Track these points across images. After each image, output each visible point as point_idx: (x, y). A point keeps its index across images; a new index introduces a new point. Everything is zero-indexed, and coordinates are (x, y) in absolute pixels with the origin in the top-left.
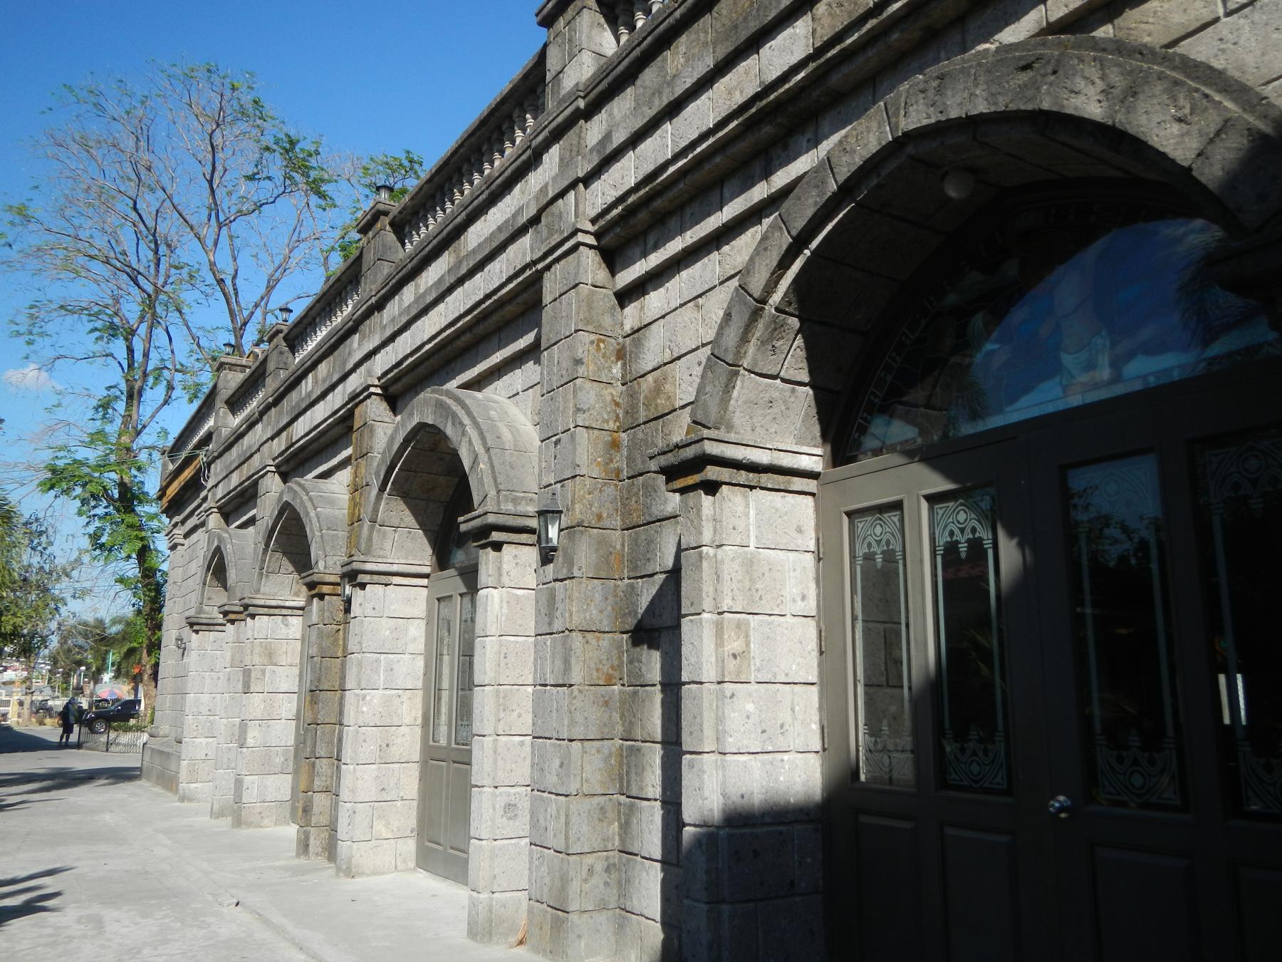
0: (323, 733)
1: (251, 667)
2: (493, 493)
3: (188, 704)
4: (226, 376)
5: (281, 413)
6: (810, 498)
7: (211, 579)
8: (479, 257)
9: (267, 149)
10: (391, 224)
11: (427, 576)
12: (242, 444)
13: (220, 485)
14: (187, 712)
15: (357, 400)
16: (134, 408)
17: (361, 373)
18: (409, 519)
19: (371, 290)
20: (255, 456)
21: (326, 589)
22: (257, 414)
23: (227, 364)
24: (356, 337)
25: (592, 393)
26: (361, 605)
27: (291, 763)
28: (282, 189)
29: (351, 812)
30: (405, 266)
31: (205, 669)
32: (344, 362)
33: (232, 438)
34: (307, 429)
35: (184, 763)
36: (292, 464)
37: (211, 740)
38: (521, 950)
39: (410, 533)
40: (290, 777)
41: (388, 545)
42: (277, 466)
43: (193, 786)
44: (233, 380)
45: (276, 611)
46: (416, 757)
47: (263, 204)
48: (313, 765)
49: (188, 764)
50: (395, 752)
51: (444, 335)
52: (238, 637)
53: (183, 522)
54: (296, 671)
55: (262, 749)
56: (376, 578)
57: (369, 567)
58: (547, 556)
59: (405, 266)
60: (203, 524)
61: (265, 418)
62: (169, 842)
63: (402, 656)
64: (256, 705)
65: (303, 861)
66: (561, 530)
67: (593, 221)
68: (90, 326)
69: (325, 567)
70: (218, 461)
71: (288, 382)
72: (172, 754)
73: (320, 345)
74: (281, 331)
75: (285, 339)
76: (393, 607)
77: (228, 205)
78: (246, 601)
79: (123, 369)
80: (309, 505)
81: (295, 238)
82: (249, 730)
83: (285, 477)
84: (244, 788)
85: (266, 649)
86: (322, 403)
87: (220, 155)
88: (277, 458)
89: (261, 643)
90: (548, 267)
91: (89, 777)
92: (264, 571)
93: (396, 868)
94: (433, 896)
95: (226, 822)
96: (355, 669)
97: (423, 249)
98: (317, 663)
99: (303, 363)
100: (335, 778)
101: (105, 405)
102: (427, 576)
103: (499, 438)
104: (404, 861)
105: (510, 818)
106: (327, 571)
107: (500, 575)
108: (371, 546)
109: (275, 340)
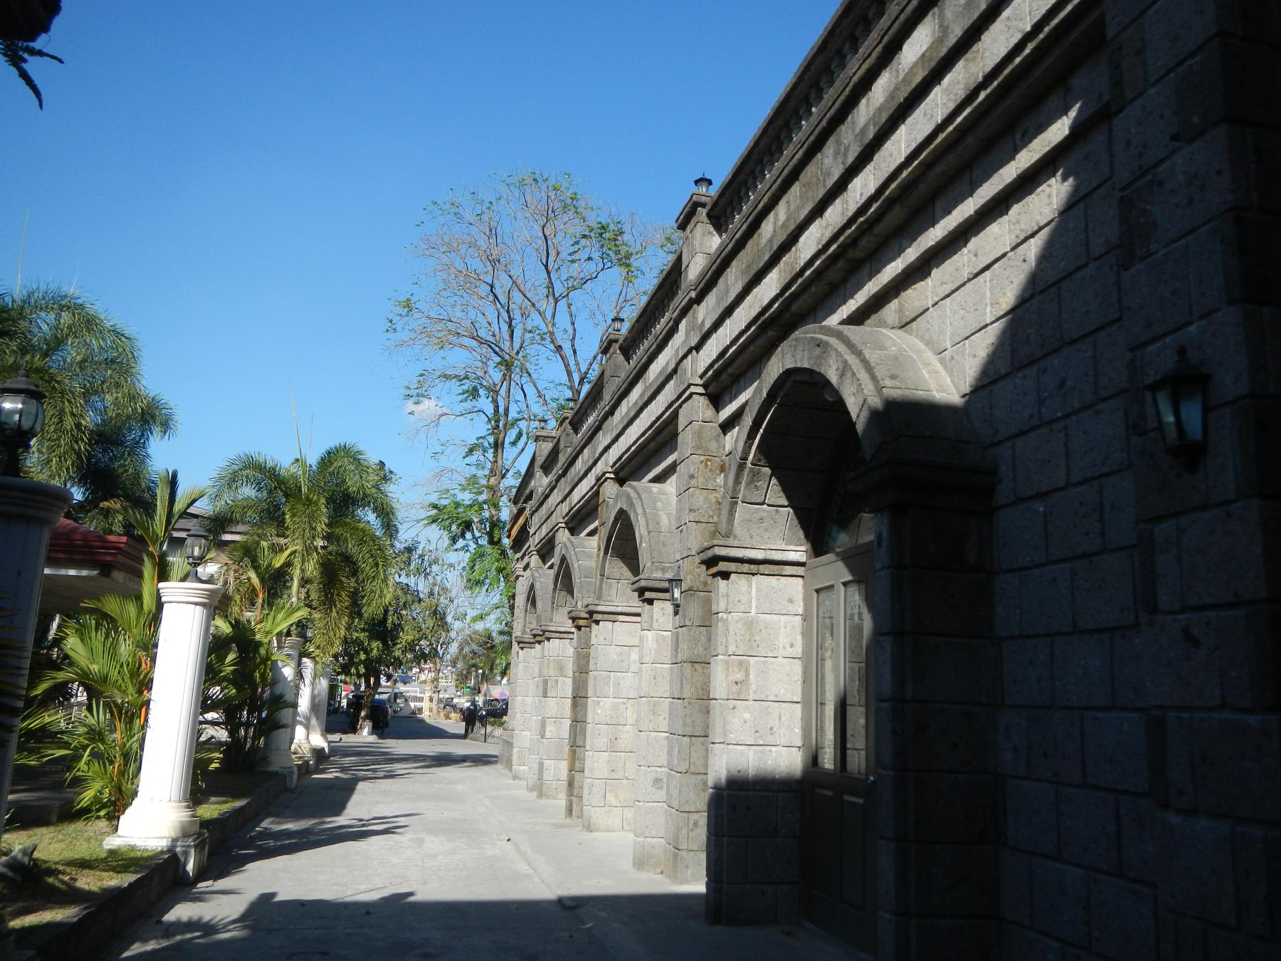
6: (800, 579)
10: (620, 348)
13: (537, 534)
23: (541, 436)
25: (701, 498)
34: (579, 498)
35: (515, 750)
38: (660, 877)
41: (614, 592)
43: (522, 768)
45: (565, 636)
56: (606, 616)
57: (600, 608)
58: (677, 607)
63: (626, 674)
64: (551, 707)
65: (568, 821)
66: (682, 593)
67: (701, 377)
70: (536, 514)
74: (567, 418)
75: (570, 423)
76: (619, 638)
84: (544, 769)
85: (558, 664)
89: (555, 660)
90: (680, 406)
91: (462, 759)
95: (535, 794)
103: (657, 524)
105: (657, 788)
107: (652, 621)
108: (602, 593)
109: (564, 424)
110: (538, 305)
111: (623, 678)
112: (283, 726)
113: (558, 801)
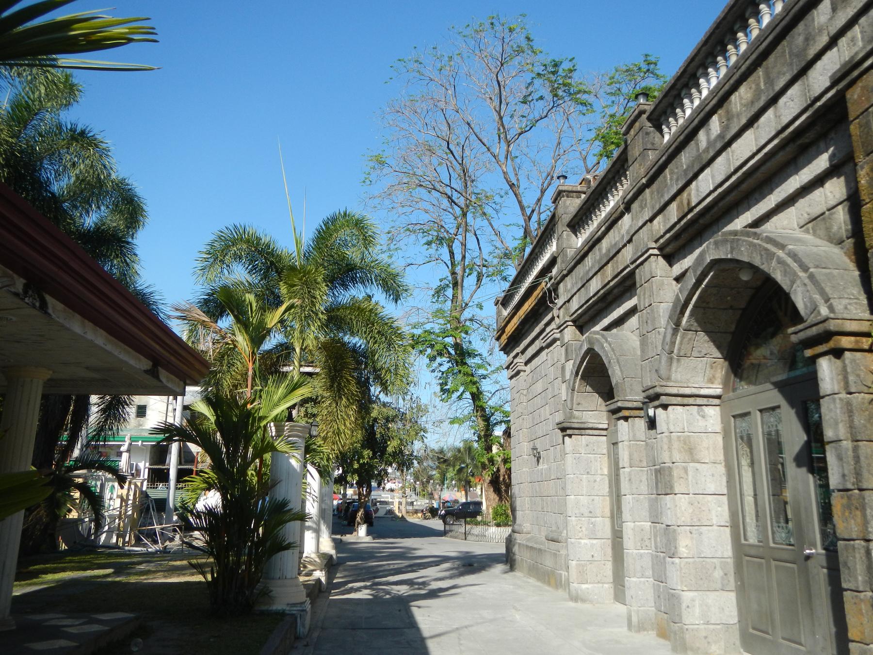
1: (671, 465)
3: (570, 505)
4: (565, 202)
7: (580, 384)
12: (600, 249)
15: (856, 73)
16: (459, 291)
22: (622, 207)
23: (564, 191)
27: (732, 578)
33: (586, 248)
36: (684, 237)
37: (595, 541)
40: (732, 596)
43: (584, 586)
44: (572, 205)
45: (691, 401)
49: (576, 565)
52: (634, 435)
53: (523, 352)
60: (554, 341)
61: (635, 206)
64: (683, 508)
68: (425, 240)
70: (568, 279)
71: (674, 146)
72: (545, 551)
74: (643, 112)
75: (649, 119)
77: (514, 126)
78: (658, 390)
79: (448, 267)
80: (769, 246)
81: (556, 154)
83: (670, 259)
84: (684, 606)
85: (685, 443)
87: (504, 93)
88: (662, 237)
89: (679, 437)
98: (847, 449)
101: (439, 291)
109: (637, 124)
110: (492, 150)
112: (288, 547)
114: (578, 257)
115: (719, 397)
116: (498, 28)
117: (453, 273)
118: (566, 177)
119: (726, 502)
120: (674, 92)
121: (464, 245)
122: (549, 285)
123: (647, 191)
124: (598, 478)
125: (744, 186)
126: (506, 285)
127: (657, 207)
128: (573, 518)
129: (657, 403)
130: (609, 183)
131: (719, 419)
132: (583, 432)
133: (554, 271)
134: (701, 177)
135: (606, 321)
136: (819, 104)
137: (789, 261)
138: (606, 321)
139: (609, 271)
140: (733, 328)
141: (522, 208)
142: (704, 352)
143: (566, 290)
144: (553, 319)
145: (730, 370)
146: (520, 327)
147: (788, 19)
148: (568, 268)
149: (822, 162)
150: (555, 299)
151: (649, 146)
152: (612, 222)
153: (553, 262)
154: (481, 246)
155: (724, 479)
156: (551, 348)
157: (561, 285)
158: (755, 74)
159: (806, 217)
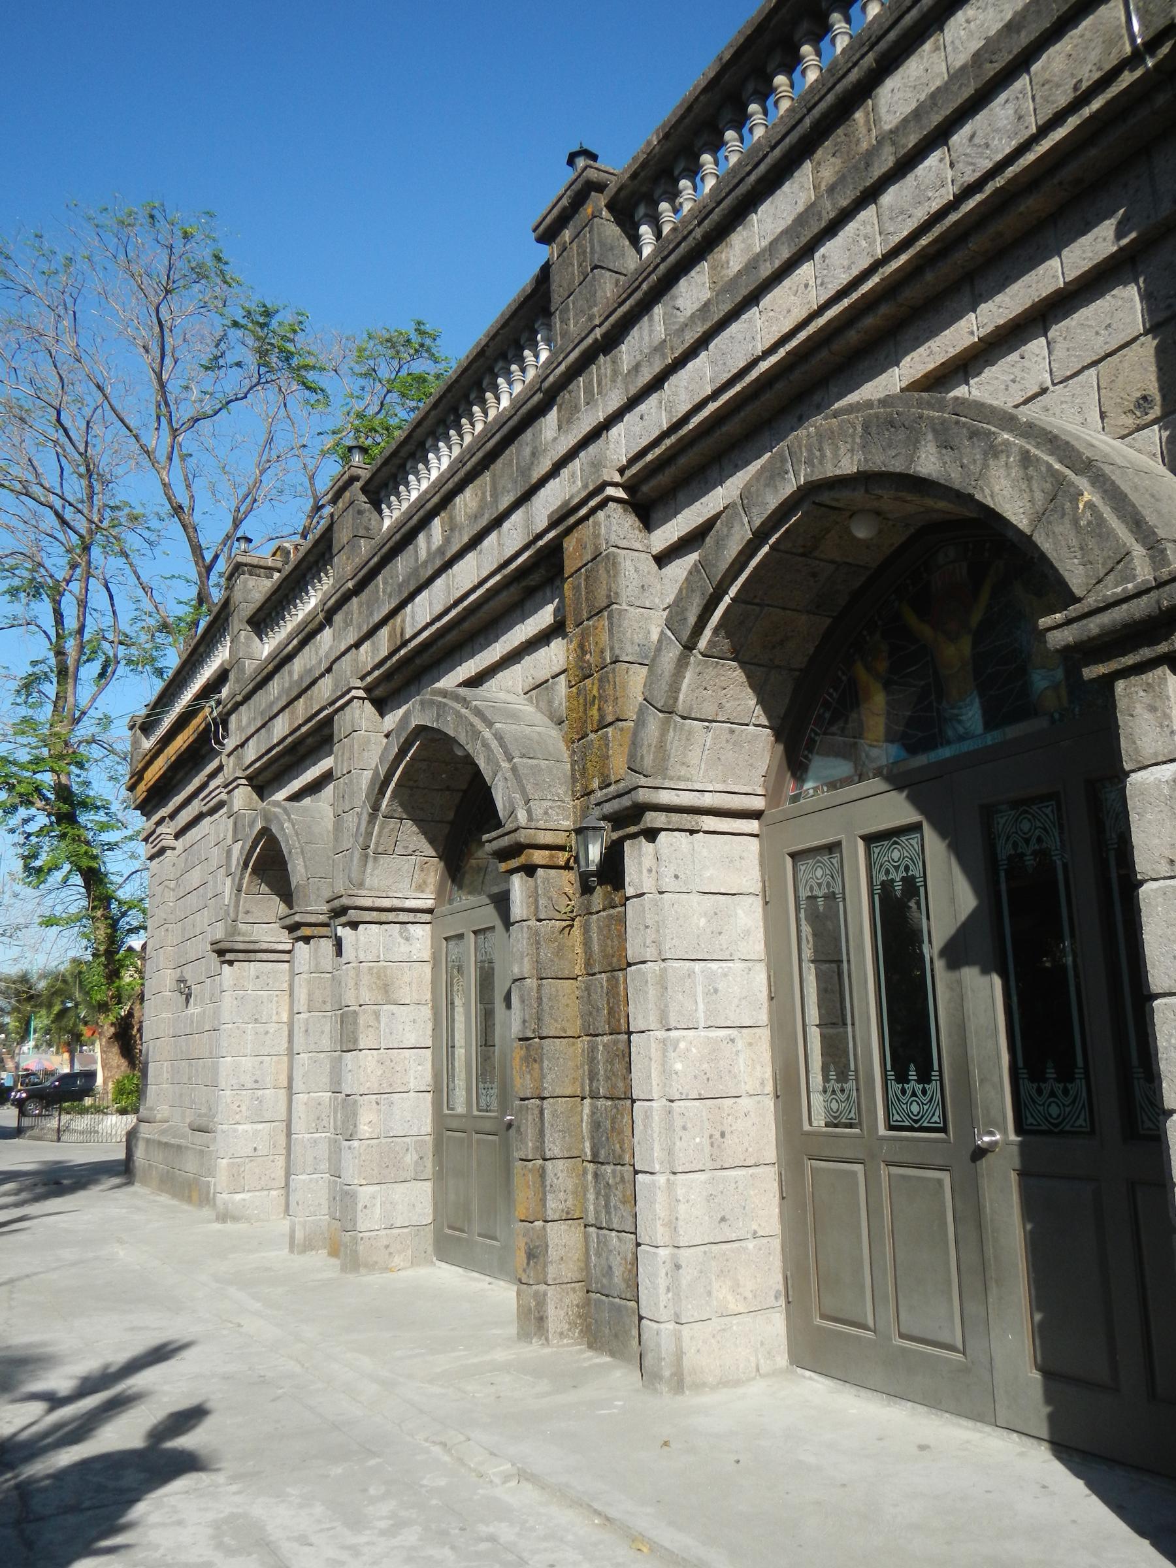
0: (554, 1114)
1: (357, 1008)
2: (1138, 551)
4: (245, 582)
5: (371, 605)
7: (250, 882)
8: (936, 119)
9: (236, 324)
10: (610, 207)
11: (756, 815)
12: (290, 673)
13: (251, 742)
14: (222, 1085)
15: (572, 520)
17: (573, 475)
18: (747, 702)
19: (591, 318)
20: (321, 682)
21: (539, 857)
22: (321, 616)
23: (246, 565)
24: (553, 415)
26: (650, 871)
27: (429, 1162)
28: (255, 380)
29: (669, 1265)
30: (685, 238)
31: (246, 1019)
32: (525, 471)
33: (270, 667)
34: (439, 609)
36: (398, 679)
37: (260, 1126)
39: (732, 731)
40: (428, 1187)
41: (694, 756)
42: (367, 689)
43: (238, 1197)
44: (256, 589)
45: (391, 916)
46: (771, 1154)
47: (231, 401)
48: (542, 1173)
49: (229, 1165)
50: (734, 1148)
51: (821, 321)
52: (317, 964)
53: (172, 816)
54: (426, 1012)
55: (384, 1141)
56: (676, 819)
57: (665, 797)
59: (685, 238)
60: (221, 805)
61: (338, 618)
62: (258, 1305)
63: (730, 964)
65: (534, 1350)
69: (530, 819)
70: (243, 709)
71: (388, 546)
72: (187, 1148)
73: (453, 470)
74: (357, 478)
75: (364, 490)
78: (345, 901)
79: (49, 639)
80: (476, 721)
81: (264, 458)
82: (361, 1111)
83: (382, 705)
84: (360, 1206)
85: (379, 978)
86: (471, 557)
87: (169, 340)
88: (369, 673)
89: (370, 969)
92: (370, 851)
93: (758, 1370)
94: (922, 1448)
96: (652, 992)
97: (742, 180)
98: (531, 989)
99: (398, 526)
100: (591, 1196)
101: (29, 684)
102: (756, 815)
104: (770, 1355)
106: (533, 825)
109: (347, 494)
110: (144, 441)
111: (725, 975)
113: (395, 1275)
114: (259, 678)
115: (430, 911)
116: (163, 225)
117: (60, 653)
118: (249, 541)
119: (430, 1059)
120: (397, 461)
121: (83, 604)
122: (215, 714)
123: (355, 600)
124: (272, 1028)
125: (466, 625)
126: (159, 685)
127: (365, 629)
128: (228, 1093)
129: (343, 919)
130: (309, 569)
131: (429, 942)
132: (252, 956)
133: (225, 692)
134: (418, 599)
135: (296, 785)
136: (541, 543)
137: (494, 744)
138: (296, 785)
139: (301, 709)
140: (451, 815)
141: (197, 550)
142: (412, 848)
143: (240, 728)
144: (220, 768)
145: (446, 874)
146: (169, 774)
147: (516, 419)
148: (244, 693)
149: (544, 617)
150: (224, 738)
151: (362, 532)
152: (307, 635)
153: (222, 677)
154: (117, 607)
155: (430, 1026)
156: (216, 816)
157: (233, 718)
158: (481, 477)
159: (530, 683)
